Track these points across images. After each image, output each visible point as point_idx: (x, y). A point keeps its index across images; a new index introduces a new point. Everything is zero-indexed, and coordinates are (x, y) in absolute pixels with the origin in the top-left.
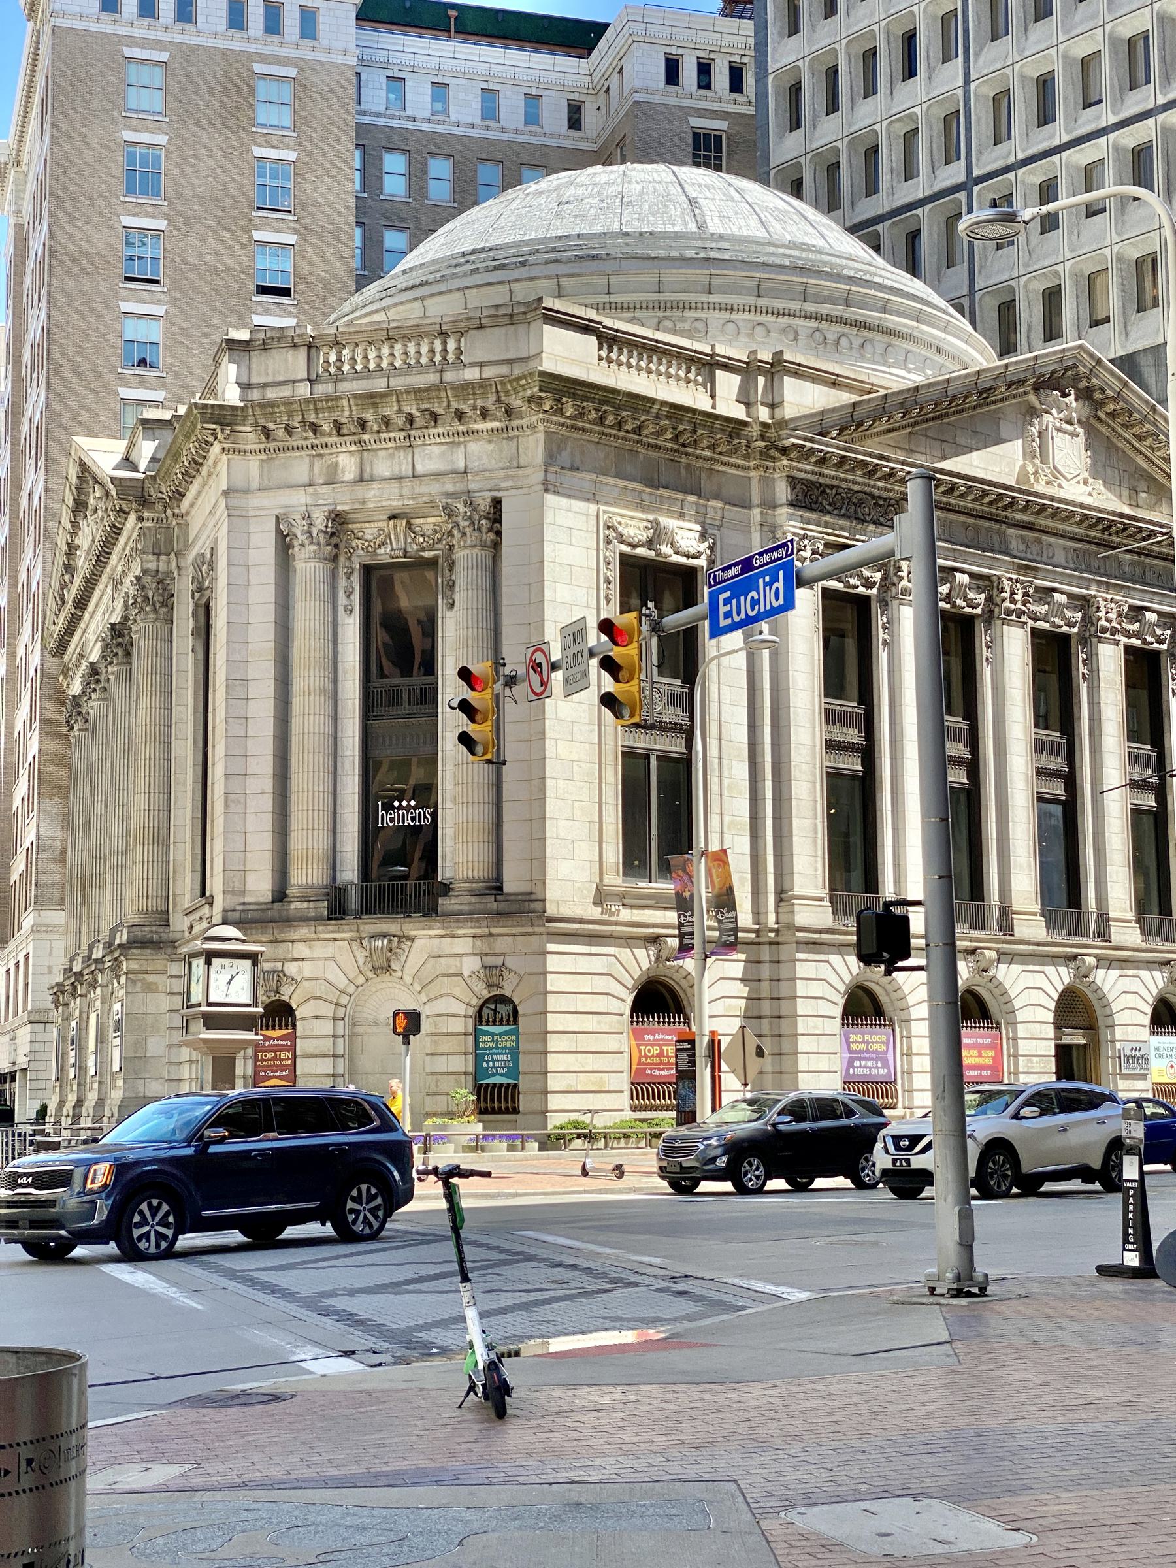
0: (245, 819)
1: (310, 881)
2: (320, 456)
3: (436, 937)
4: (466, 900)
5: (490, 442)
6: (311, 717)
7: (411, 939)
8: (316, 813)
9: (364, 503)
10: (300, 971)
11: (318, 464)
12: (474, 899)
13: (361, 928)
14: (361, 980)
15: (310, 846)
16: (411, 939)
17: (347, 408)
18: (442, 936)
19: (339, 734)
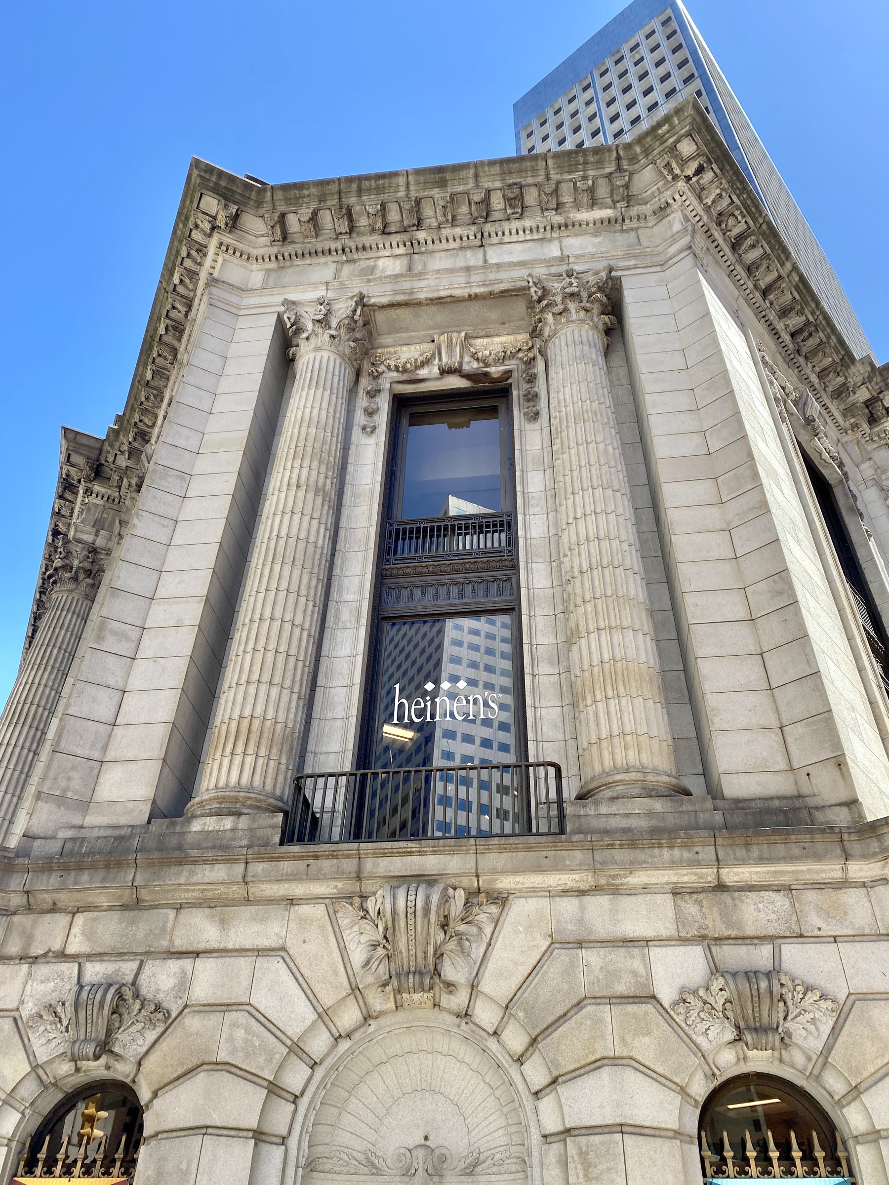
0: (131, 667)
1: (245, 780)
2: (354, 261)
3: (566, 892)
4: (639, 806)
5: (596, 234)
6: (297, 517)
7: (501, 899)
8: (281, 658)
9: (412, 293)
10: (184, 983)
11: (346, 270)
12: (658, 805)
13: (369, 865)
14: (349, 1016)
15: (259, 711)
16: (501, 899)
17: (402, 188)
18: (581, 893)
19: (337, 571)
